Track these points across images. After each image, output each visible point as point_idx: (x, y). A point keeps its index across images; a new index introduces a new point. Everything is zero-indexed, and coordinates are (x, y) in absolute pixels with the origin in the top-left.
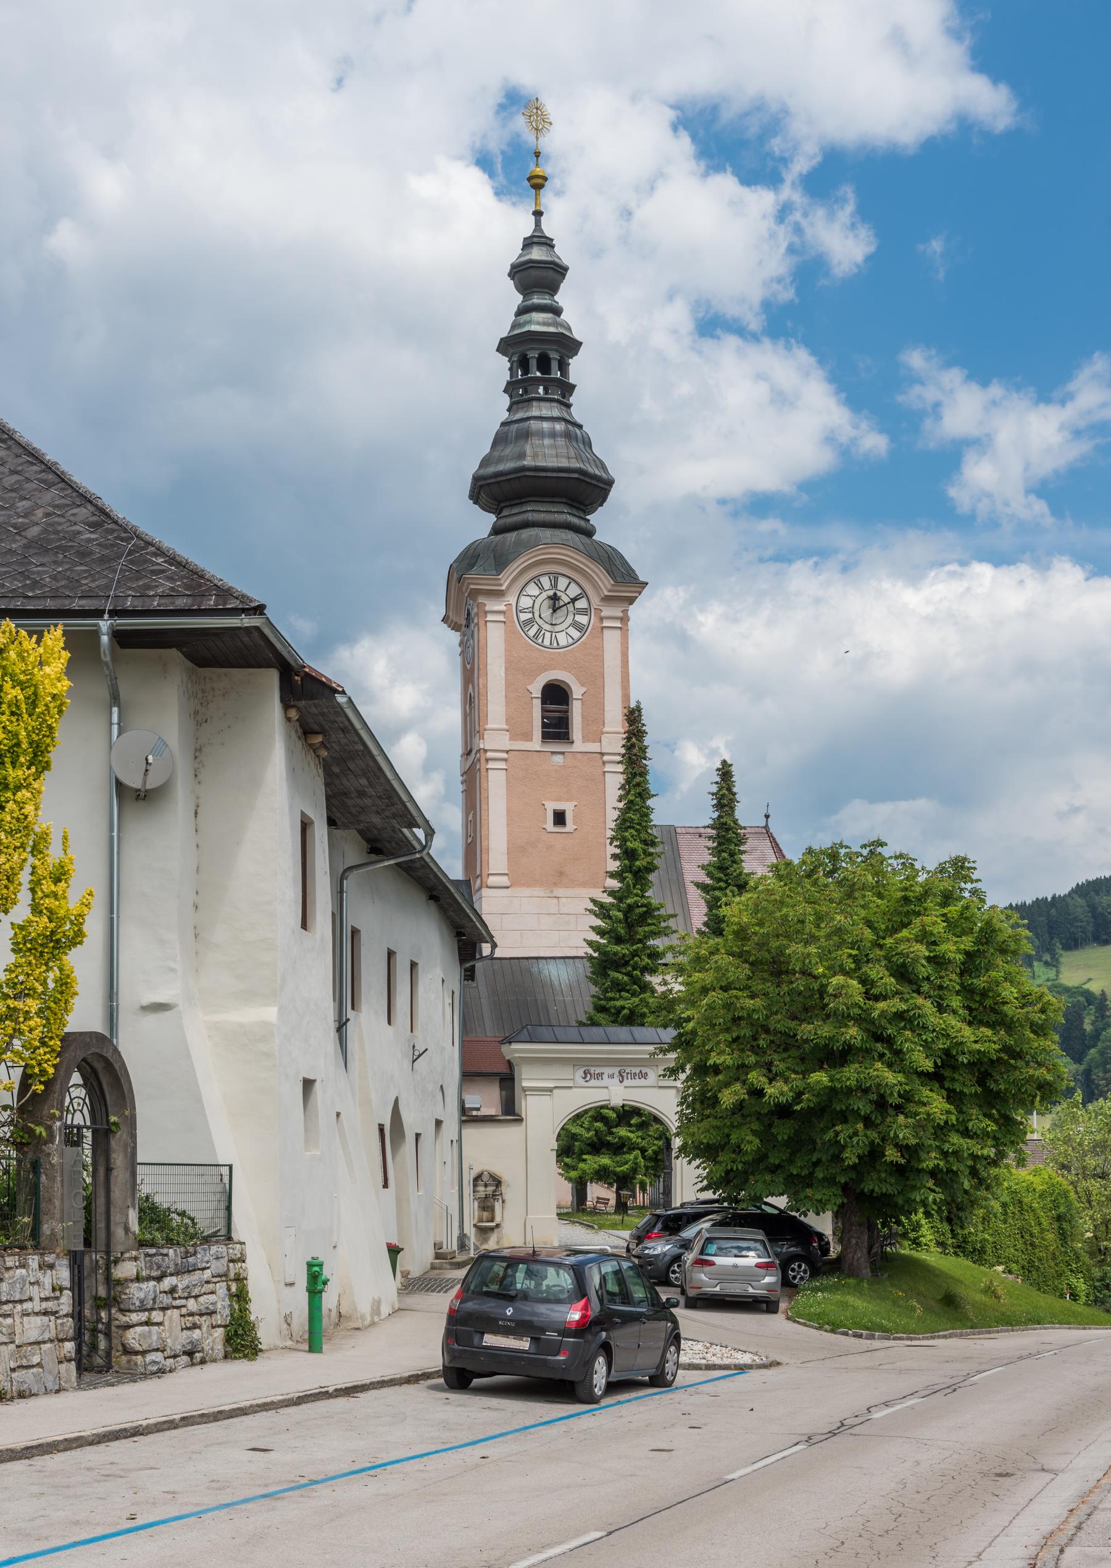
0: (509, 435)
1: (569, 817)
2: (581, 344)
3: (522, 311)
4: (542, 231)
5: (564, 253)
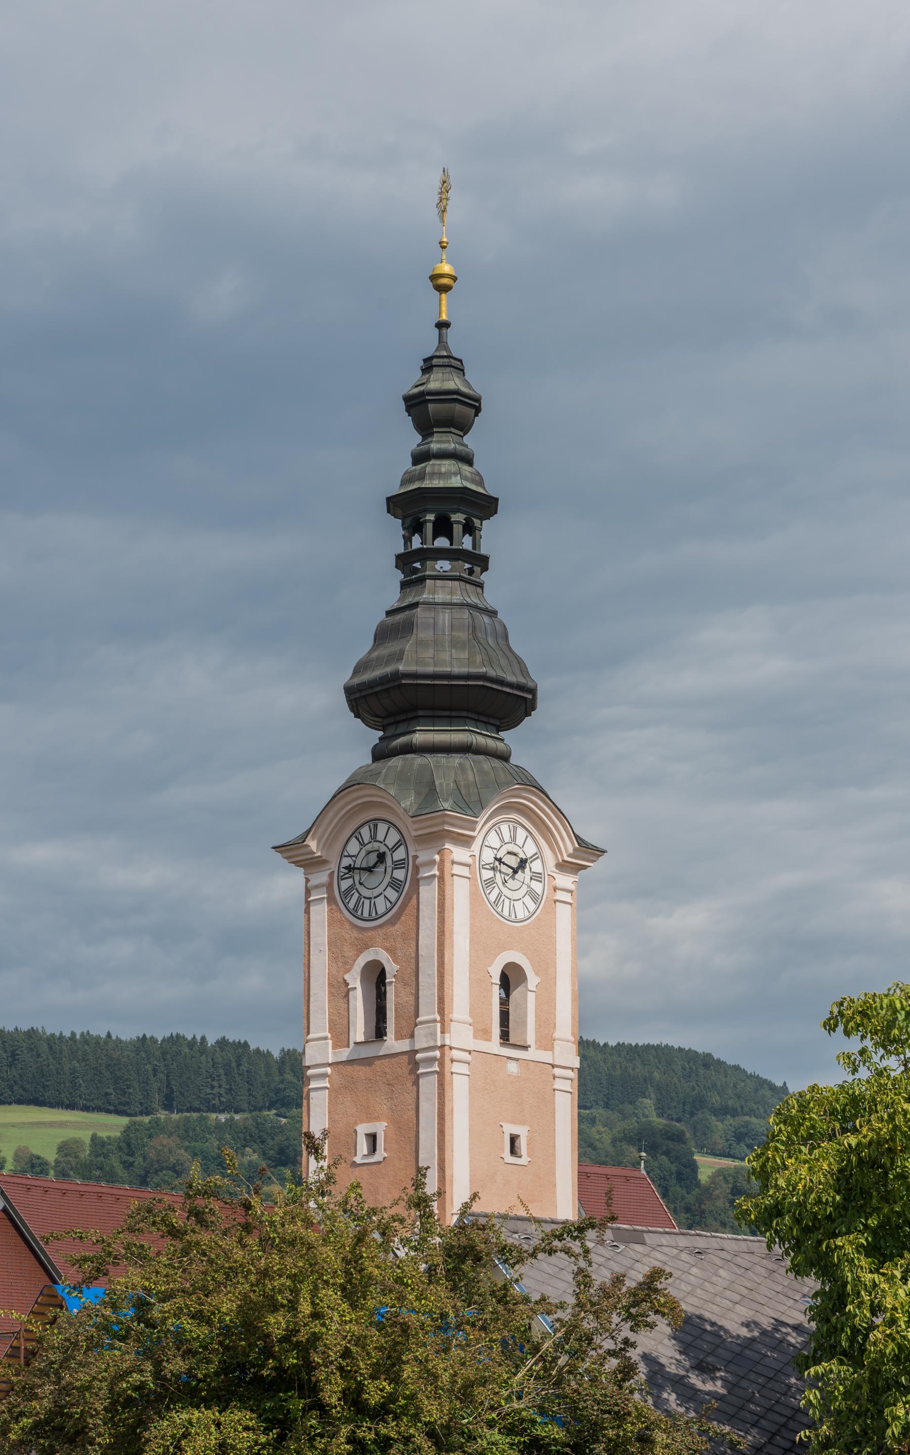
0: (395, 627)
2: (497, 500)
3: (420, 457)
4: (446, 348)
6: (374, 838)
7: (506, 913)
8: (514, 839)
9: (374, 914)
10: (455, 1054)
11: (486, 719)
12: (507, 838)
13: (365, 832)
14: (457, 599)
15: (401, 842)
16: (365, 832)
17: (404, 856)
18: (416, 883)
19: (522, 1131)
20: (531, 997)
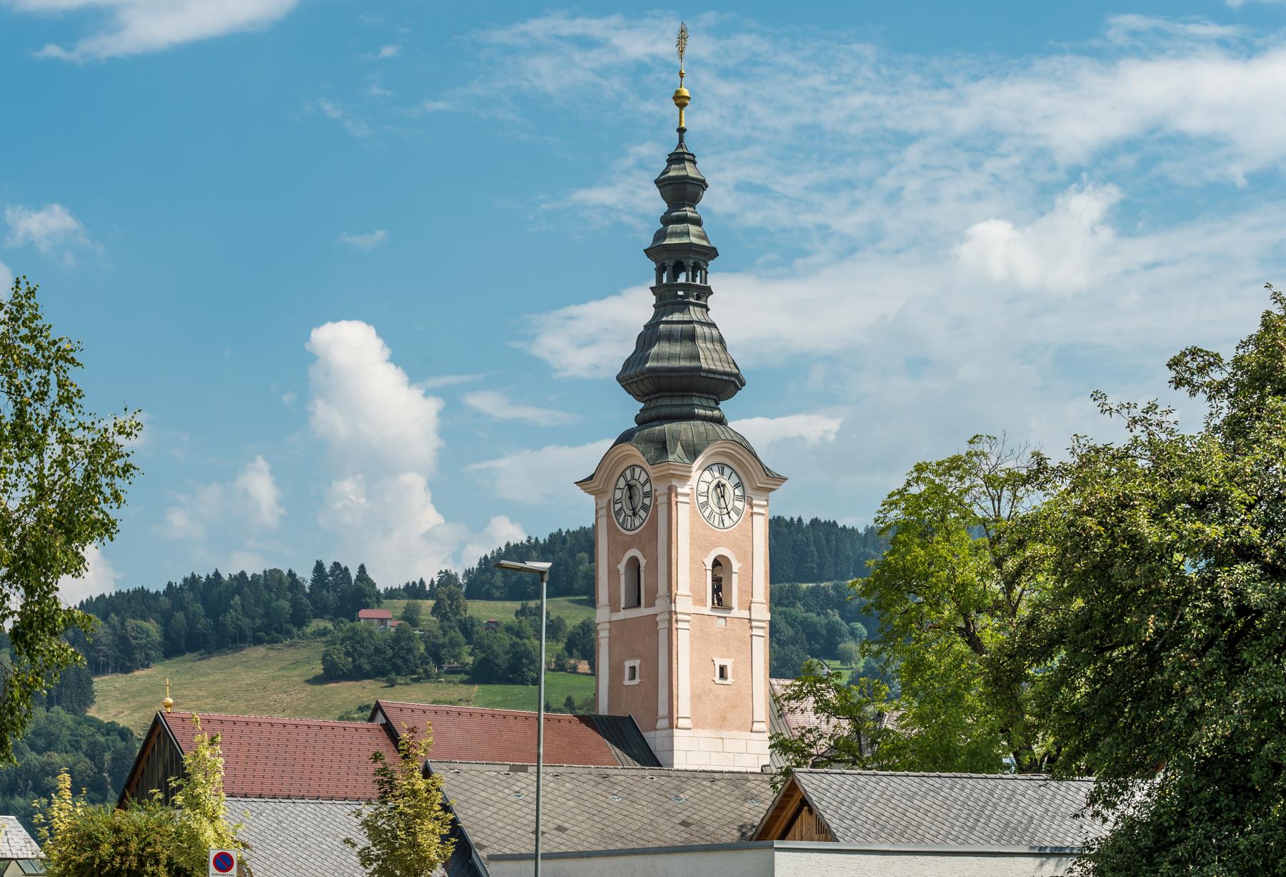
1: (729, 672)
3: (666, 220)
6: (633, 477)
10: (680, 617)
13: (628, 473)
14: (686, 318)
15: (648, 480)
16: (628, 473)
18: (656, 506)
19: (728, 663)
20: (735, 578)
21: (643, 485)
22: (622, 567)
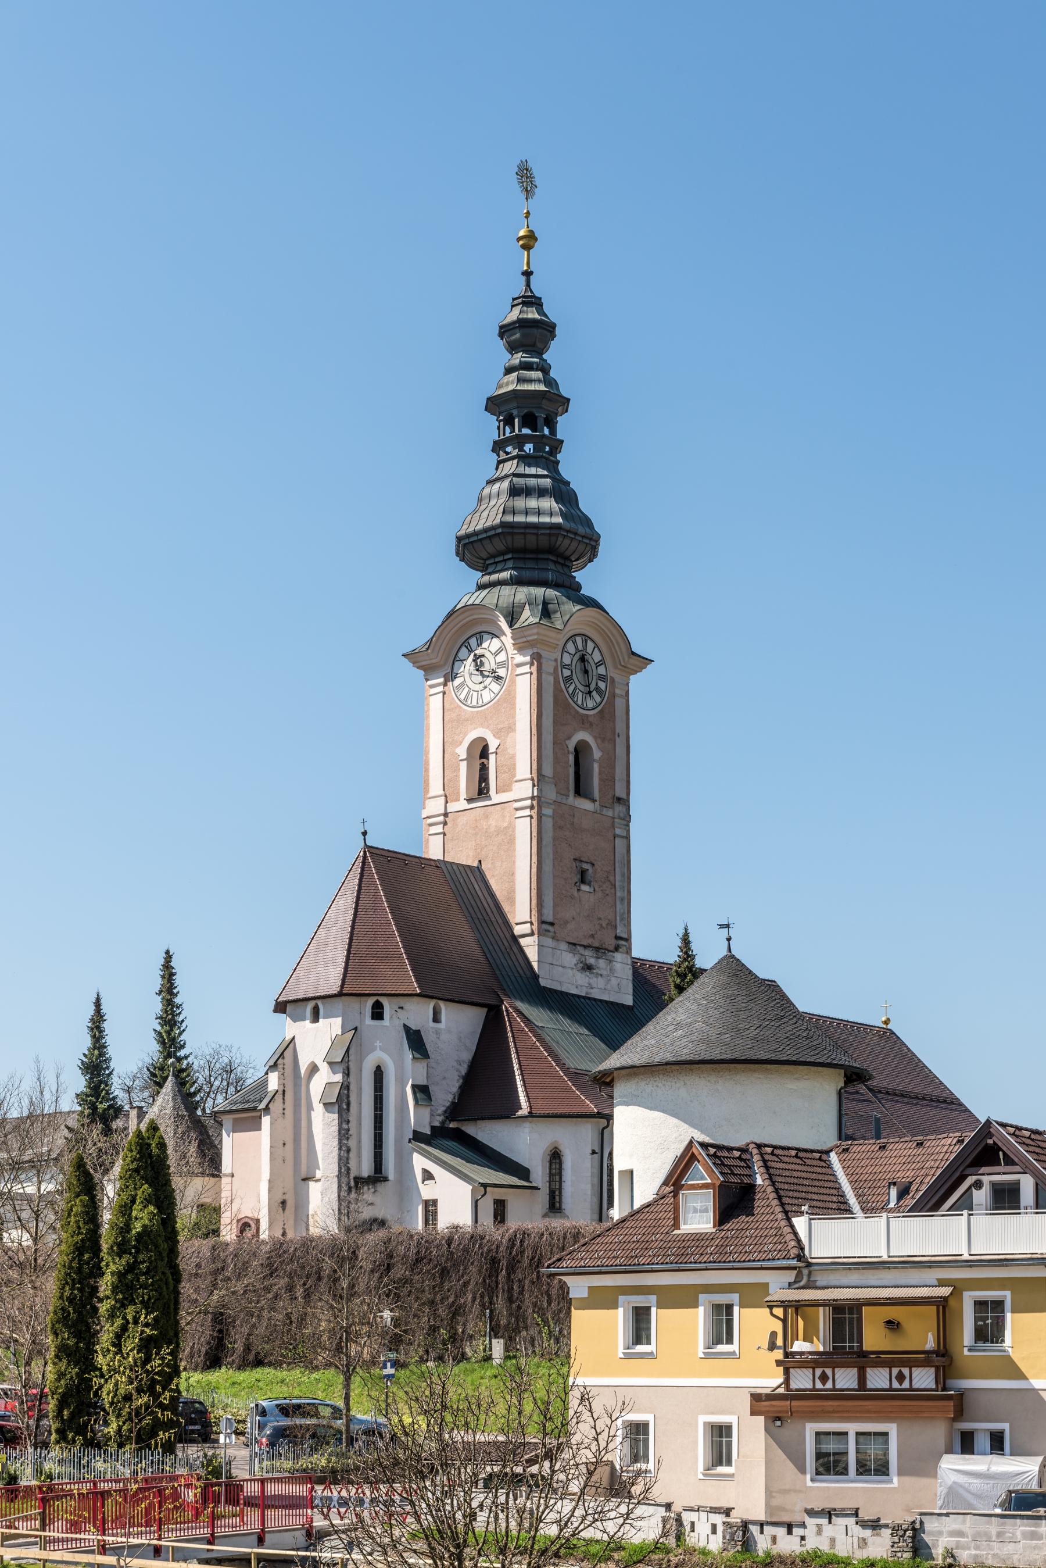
2: (568, 400)
4: (531, 291)
5: (553, 311)
7: (580, 702)
8: (585, 647)
9: (480, 703)
11: (562, 561)
12: (580, 648)
17: (505, 658)
21: (497, 653)
22: (462, 752)
